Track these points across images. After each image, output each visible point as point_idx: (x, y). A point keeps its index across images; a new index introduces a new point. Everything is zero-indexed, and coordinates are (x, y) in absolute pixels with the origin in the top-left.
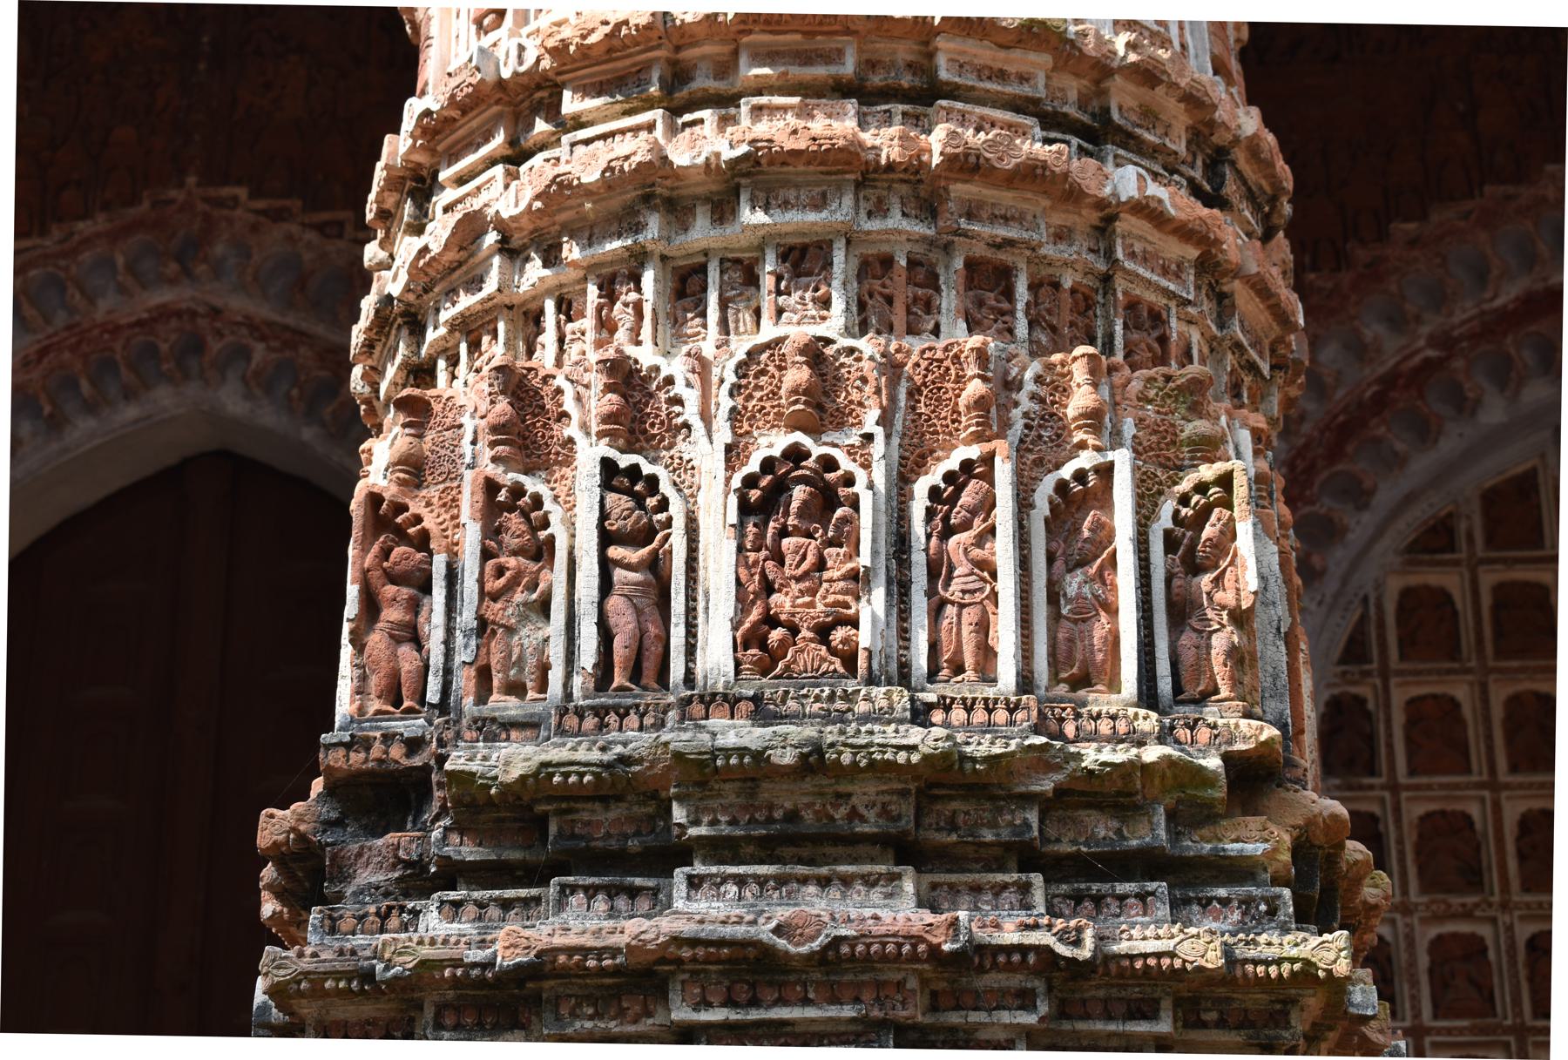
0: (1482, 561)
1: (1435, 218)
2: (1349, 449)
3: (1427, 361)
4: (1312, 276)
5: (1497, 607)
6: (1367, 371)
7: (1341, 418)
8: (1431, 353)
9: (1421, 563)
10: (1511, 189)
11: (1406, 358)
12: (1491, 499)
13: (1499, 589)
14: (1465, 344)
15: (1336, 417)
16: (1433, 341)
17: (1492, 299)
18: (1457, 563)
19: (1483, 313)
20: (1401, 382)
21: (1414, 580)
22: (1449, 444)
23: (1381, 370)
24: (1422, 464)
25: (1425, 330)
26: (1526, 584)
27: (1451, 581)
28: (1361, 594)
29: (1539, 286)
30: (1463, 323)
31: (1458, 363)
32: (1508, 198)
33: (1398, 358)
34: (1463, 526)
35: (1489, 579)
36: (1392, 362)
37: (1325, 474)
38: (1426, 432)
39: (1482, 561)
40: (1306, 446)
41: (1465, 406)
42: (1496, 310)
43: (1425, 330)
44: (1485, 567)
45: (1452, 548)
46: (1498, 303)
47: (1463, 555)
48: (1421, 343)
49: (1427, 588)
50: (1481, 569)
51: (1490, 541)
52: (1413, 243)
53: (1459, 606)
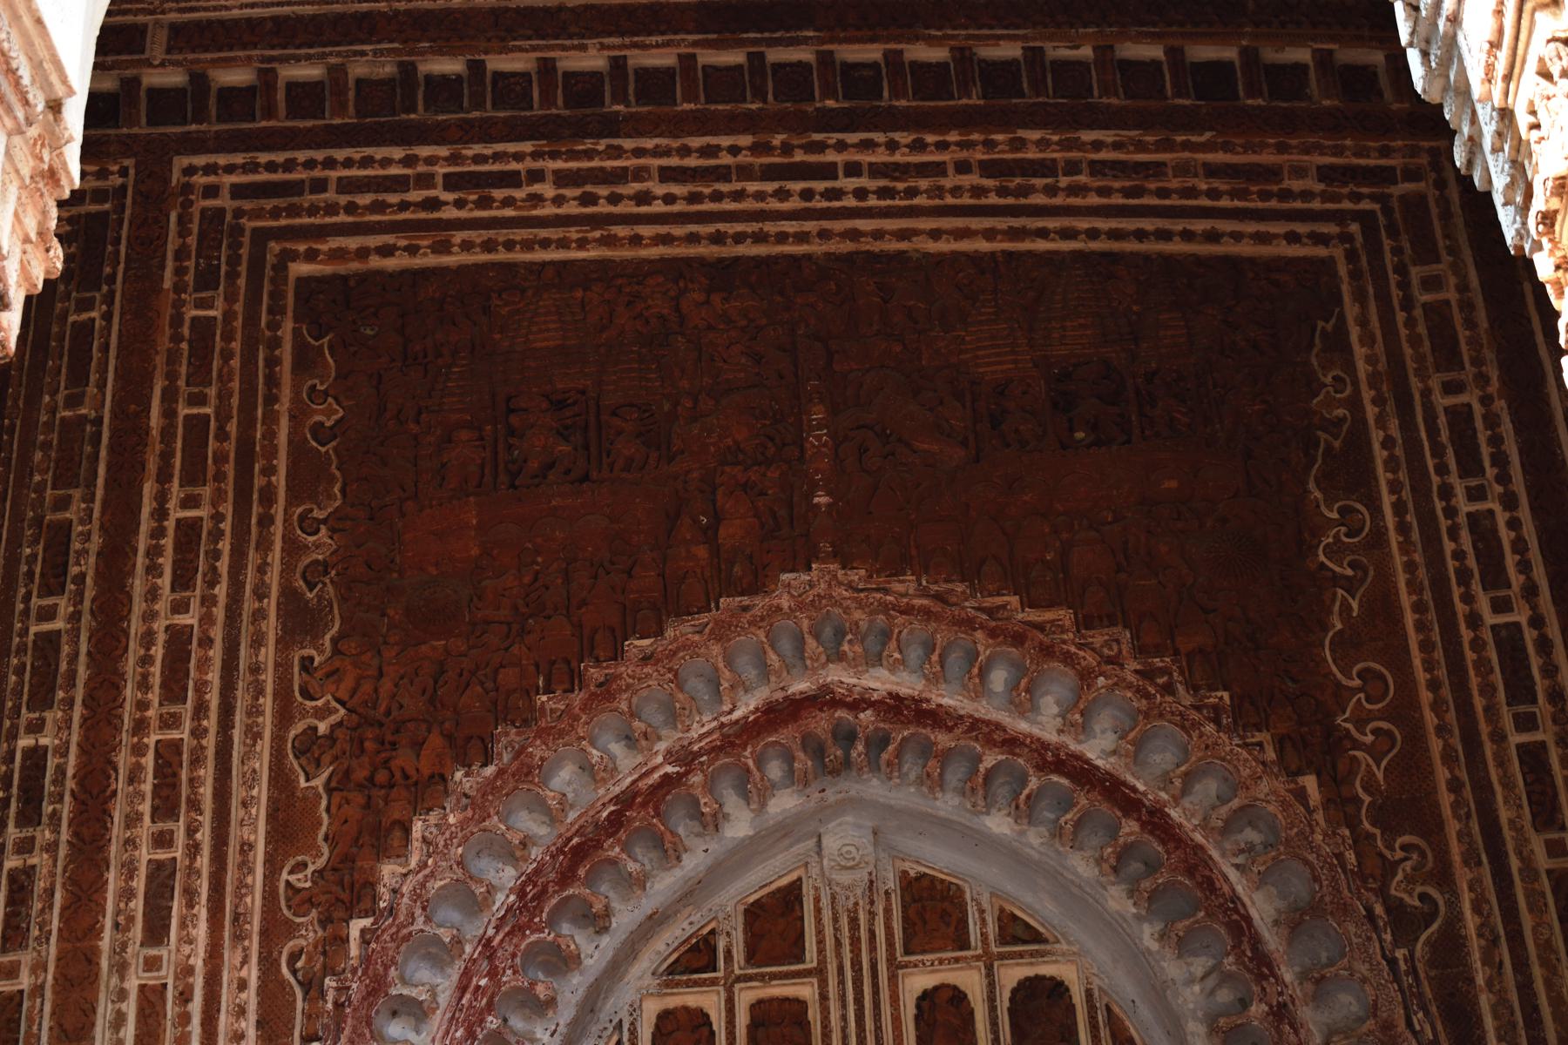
0: (739, 979)
1: (670, 633)
2: (582, 872)
3: (666, 775)
4: (544, 698)
5: (753, 1027)
6: (601, 792)
7: (575, 840)
8: (669, 769)
9: (678, 984)
10: (746, 600)
11: (641, 777)
12: (754, 913)
13: (757, 1007)
14: (704, 758)
15: (570, 839)
16: (670, 756)
17: (731, 712)
18: (714, 982)
19: (722, 725)
20: (639, 800)
21: (673, 1002)
22: (693, 862)
23: (617, 790)
24: (664, 885)
25: (662, 746)
26: (786, 1000)
27: (710, 1001)
28: (615, 1021)
29: (779, 695)
30: (702, 737)
31: (696, 779)
32: (745, 609)
33: (635, 776)
34: (721, 945)
35: (746, 997)
36: (629, 780)
37: (554, 901)
38: (670, 851)
39: (739, 979)
40: (537, 872)
41: (713, 823)
42: (737, 722)
43: (662, 746)
44: (743, 985)
45: (800, 958)
46: (737, 715)
47: (720, 974)
48: (660, 759)
49: (686, 1009)
50: (737, 986)
51: (751, 957)
52: (646, 659)
53: (715, 1027)
